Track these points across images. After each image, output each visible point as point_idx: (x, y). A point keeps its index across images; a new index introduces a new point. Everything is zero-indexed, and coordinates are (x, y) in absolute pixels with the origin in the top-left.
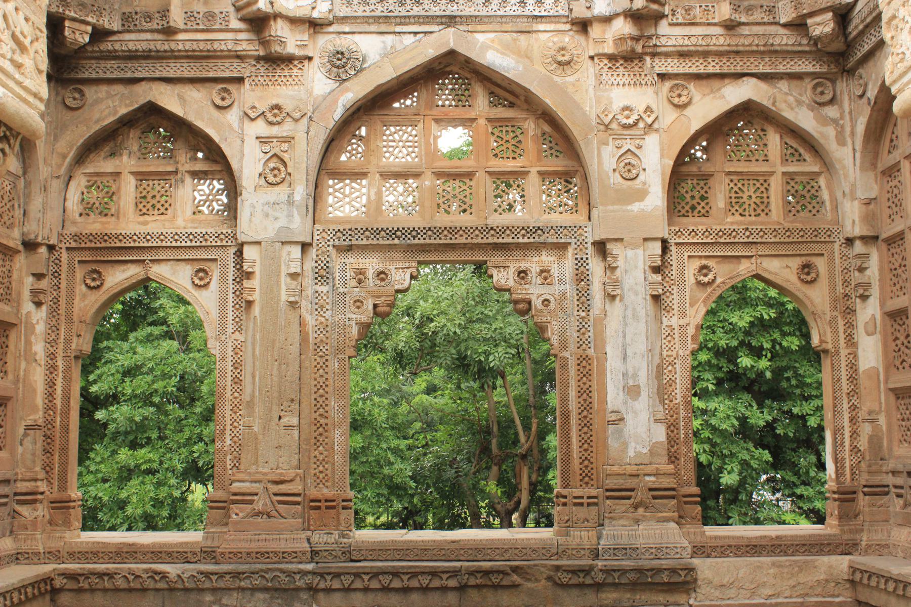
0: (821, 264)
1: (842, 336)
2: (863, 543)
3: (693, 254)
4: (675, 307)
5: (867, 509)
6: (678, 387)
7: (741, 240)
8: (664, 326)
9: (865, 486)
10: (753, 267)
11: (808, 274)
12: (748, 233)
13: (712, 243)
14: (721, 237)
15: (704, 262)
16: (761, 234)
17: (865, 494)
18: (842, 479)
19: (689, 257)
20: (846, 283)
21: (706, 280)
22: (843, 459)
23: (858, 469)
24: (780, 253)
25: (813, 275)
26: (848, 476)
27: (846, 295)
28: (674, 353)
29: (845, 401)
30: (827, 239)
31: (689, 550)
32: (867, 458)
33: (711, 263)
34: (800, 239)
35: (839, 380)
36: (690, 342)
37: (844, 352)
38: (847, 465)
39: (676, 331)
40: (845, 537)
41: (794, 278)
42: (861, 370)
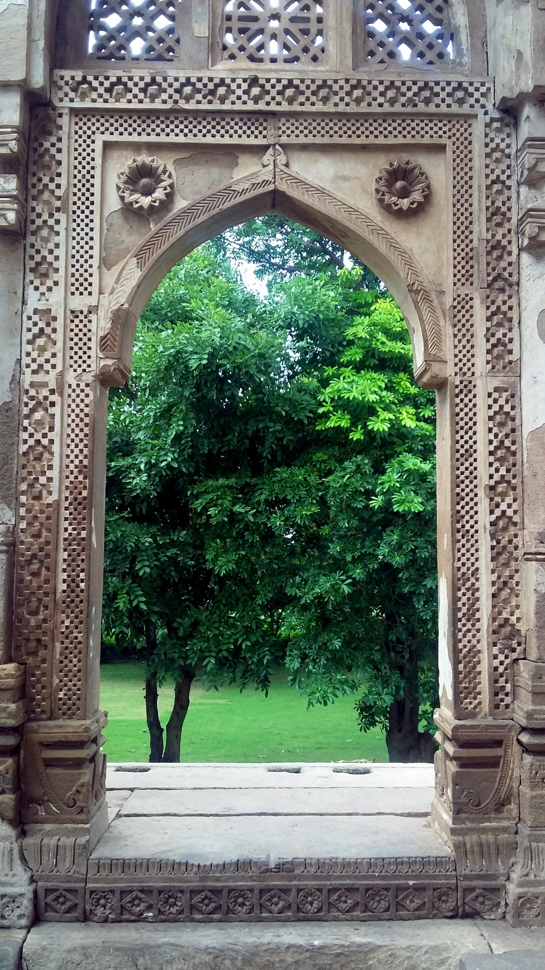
0: (438, 172)
1: (481, 346)
2: (513, 889)
3: (116, 138)
4: (60, 264)
5: (525, 790)
6: (56, 463)
7: (239, 106)
8: (29, 311)
9: (524, 729)
10: (267, 174)
11: (404, 193)
12: (256, 91)
13: (167, 113)
14: (188, 99)
15: (144, 158)
16: (289, 92)
17: (526, 749)
18: (469, 704)
19: (107, 146)
20: (496, 215)
21: (145, 201)
22: (474, 652)
23: (513, 678)
24: (336, 140)
25: (417, 196)
26: (485, 697)
27: (497, 246)
28: (51, 379)
29: (483, 505)
30: (455, 109)
31: (26, 904)
32: (533, 654)
33: (161, 162)
34: (387, 108)
35: (470, 453)
36: (95, 351)
37: (483, 385)
38: (484, 667)
39: (59, 325)
40: (468, 867)
41: (368, 205)
42: (526, 431)
